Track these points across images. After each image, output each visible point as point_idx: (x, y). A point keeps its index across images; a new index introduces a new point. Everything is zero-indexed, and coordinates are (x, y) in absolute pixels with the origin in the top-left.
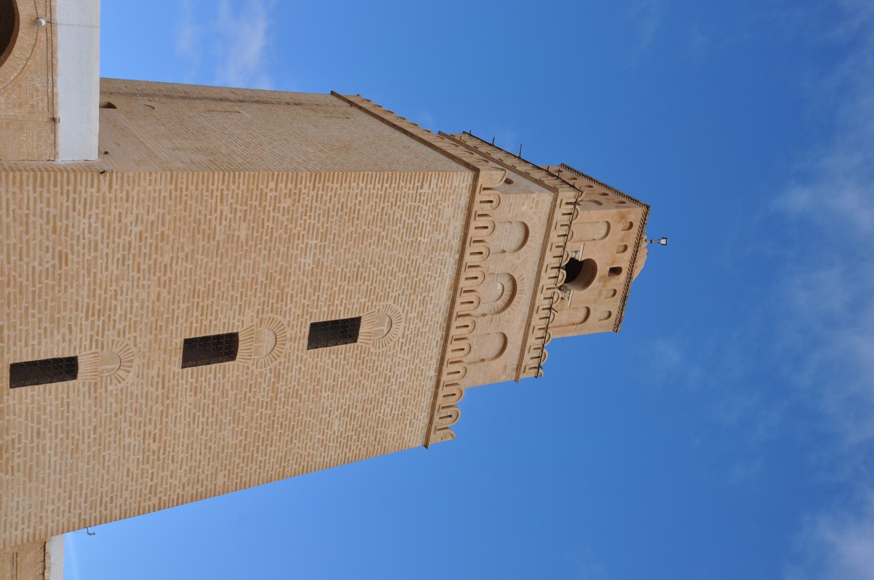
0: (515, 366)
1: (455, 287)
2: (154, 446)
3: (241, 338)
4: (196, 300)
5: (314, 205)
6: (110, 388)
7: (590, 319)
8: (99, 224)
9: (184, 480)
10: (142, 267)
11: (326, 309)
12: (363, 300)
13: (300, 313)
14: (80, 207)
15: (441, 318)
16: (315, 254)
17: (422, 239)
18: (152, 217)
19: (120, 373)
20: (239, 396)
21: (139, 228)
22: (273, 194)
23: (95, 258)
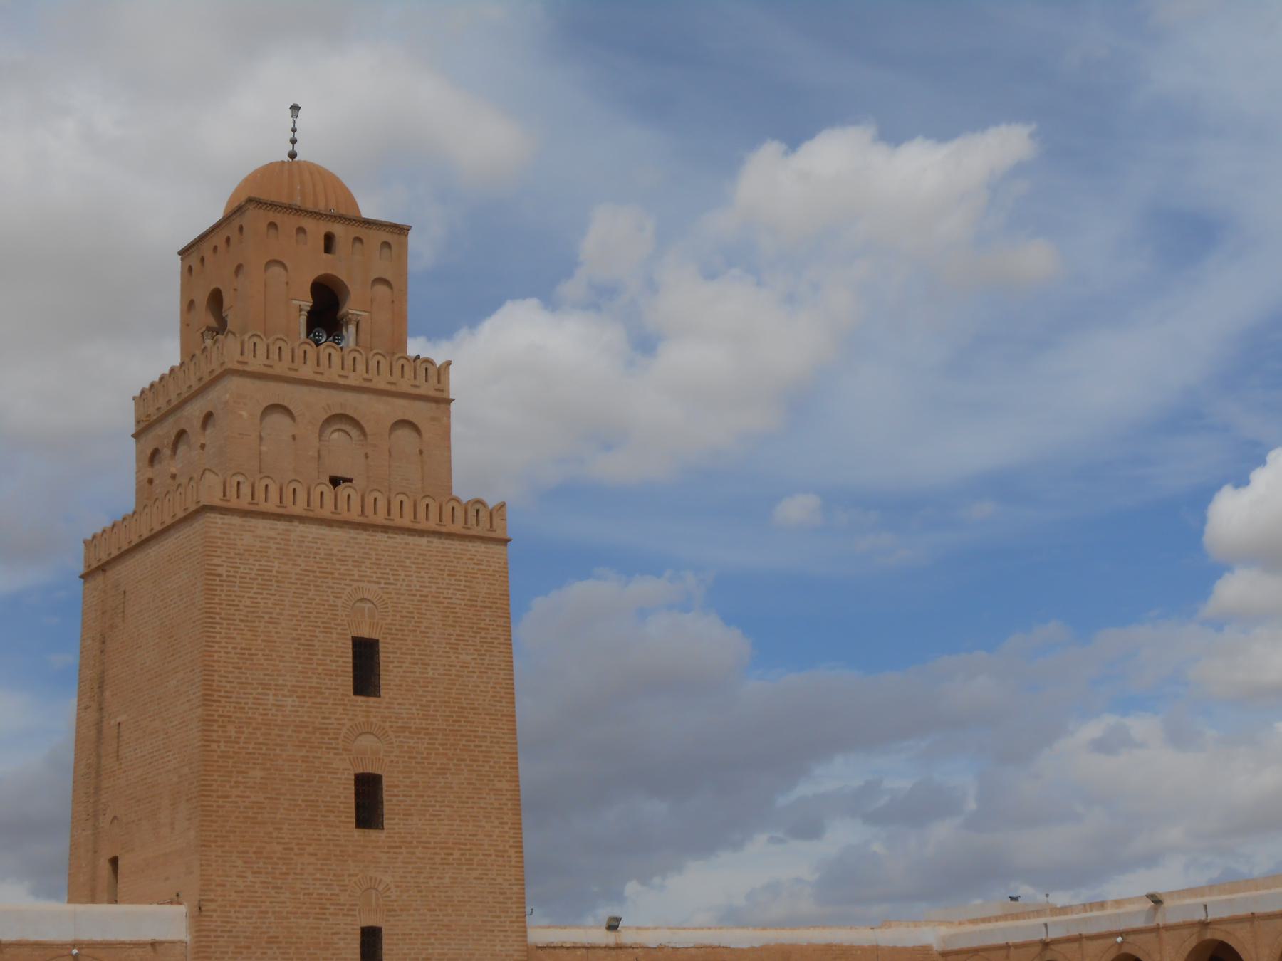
0: (433, 405)
1: (329, 523)
2: (457, 854)
3: (360, 771)
4: (319, 818)
5: (233, 700)
6: (393, 898)
7: (388, 276)
8: (244, 910)
9: (496, 823)
10: (284, 871)
11: (340, 679)
12: (335, 636)
13: (341, 708)
14: (229, 927)
15: (363, 536)
16: (284, 696)
17: (275, 569)
18: (240, 863)
19: (380, 888)
20: (419, 770)
21: (249, 874)
22: (222, 744)
23: (274, 913)
